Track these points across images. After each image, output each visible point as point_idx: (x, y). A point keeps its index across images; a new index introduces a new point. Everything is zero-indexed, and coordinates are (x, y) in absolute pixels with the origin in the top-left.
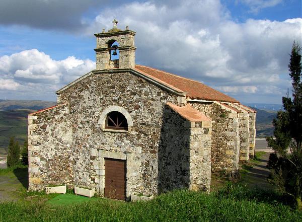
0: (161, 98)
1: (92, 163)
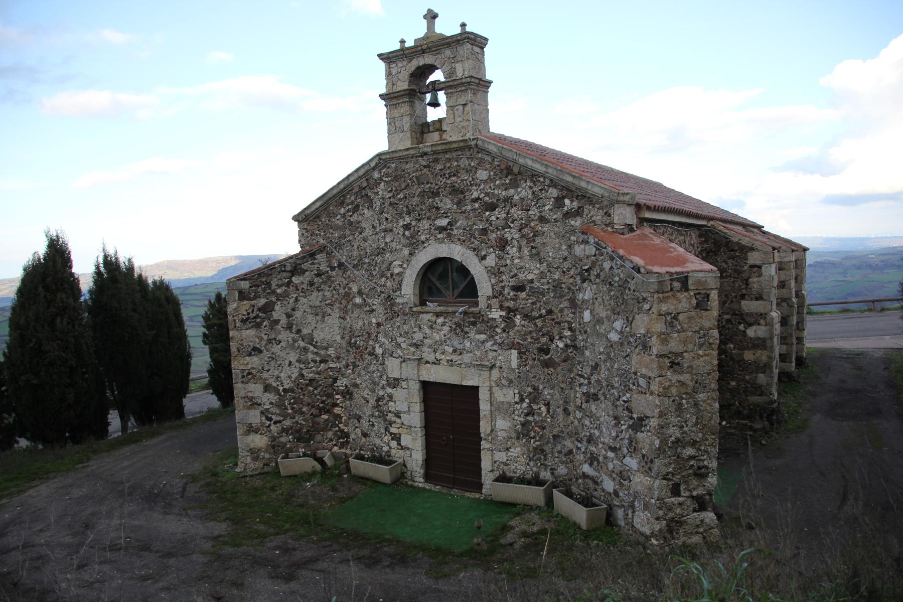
0: (568, 215)
1: (391, 397)
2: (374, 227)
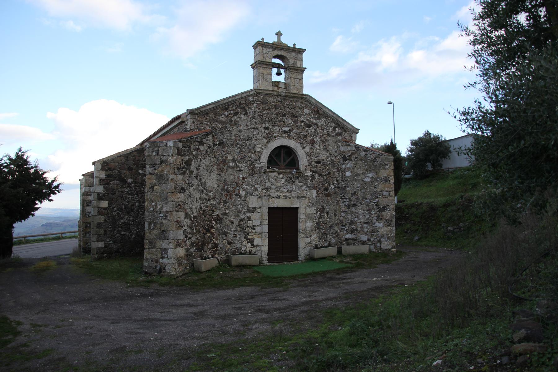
0: (337, 134)
1: (249, 219)
2: (247, 125)
